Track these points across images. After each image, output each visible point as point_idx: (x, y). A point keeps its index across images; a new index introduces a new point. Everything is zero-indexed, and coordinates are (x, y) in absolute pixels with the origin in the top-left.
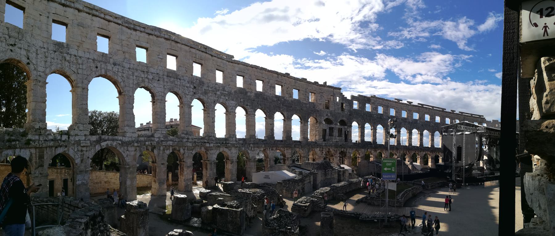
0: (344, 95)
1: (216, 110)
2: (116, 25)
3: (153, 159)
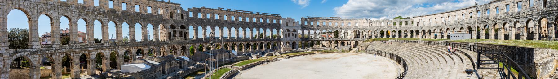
0: (183, 9)
3: (52, 61)
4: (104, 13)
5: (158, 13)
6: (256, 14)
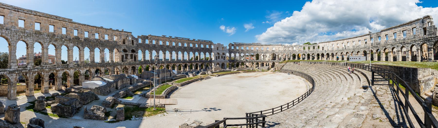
0: (133, 36)
1: (62, 49)
2: (8, 10)
3: (26, 78)
4: (70, 39)
5: (113, 40)
6: (192, 41)
